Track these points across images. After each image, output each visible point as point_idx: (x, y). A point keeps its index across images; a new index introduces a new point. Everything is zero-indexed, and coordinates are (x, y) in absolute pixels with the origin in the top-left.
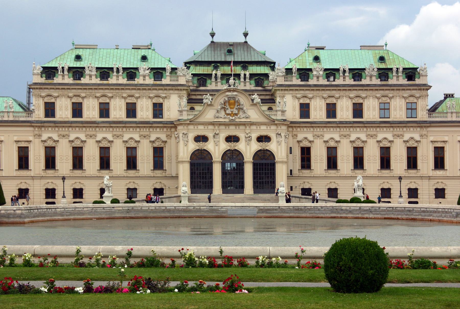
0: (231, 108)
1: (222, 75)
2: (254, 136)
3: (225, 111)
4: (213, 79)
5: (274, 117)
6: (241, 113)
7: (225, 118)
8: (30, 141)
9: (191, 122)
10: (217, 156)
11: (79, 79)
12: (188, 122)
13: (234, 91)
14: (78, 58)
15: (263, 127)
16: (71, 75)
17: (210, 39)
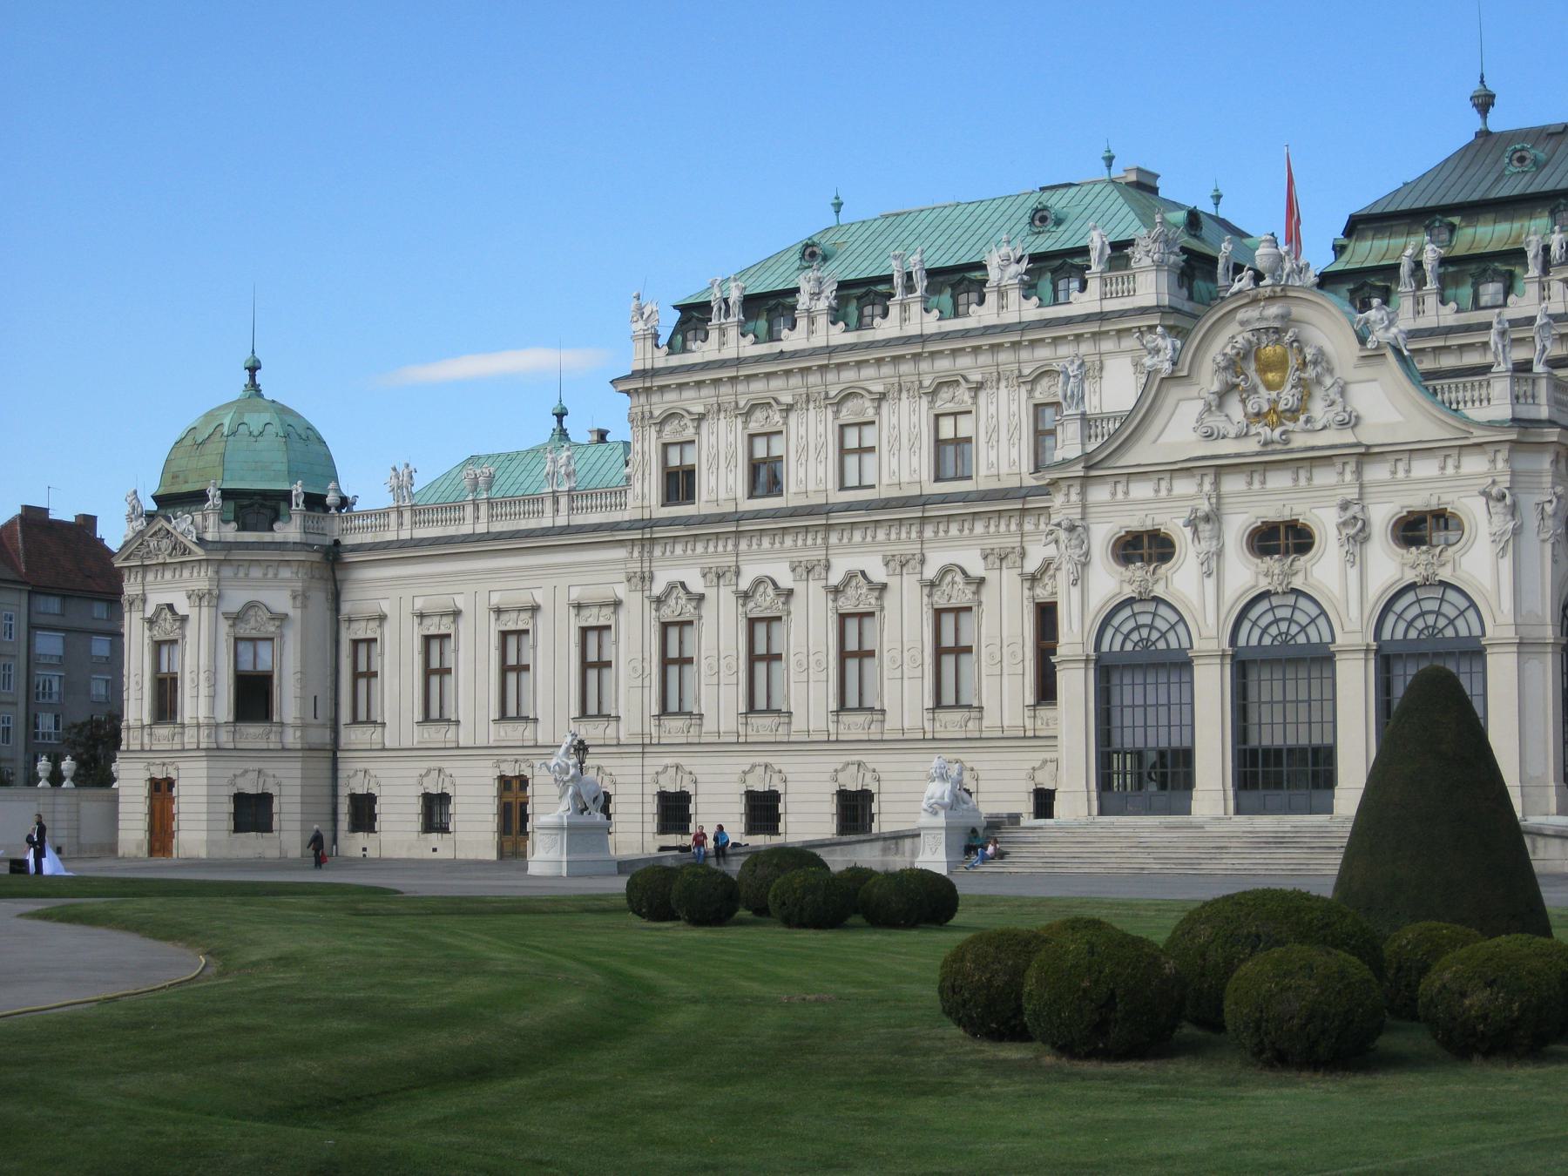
0: (1269, 387)
1: (1443, 262)
2: (1382, 515)
3: (1243, 401)
4: (1405, 286)
5: (1476, 413)
6: (1318, 409)
7: (1237, 437)
8: (617, 604)
9: (1092, 468)
10: (1207, 633)
11: (772, 337)
12: (1078, 470)
13: (1272, 298)
14: (811, 253)
15: (1425, 468)
16: (762, 324)
17: (1474, 123)
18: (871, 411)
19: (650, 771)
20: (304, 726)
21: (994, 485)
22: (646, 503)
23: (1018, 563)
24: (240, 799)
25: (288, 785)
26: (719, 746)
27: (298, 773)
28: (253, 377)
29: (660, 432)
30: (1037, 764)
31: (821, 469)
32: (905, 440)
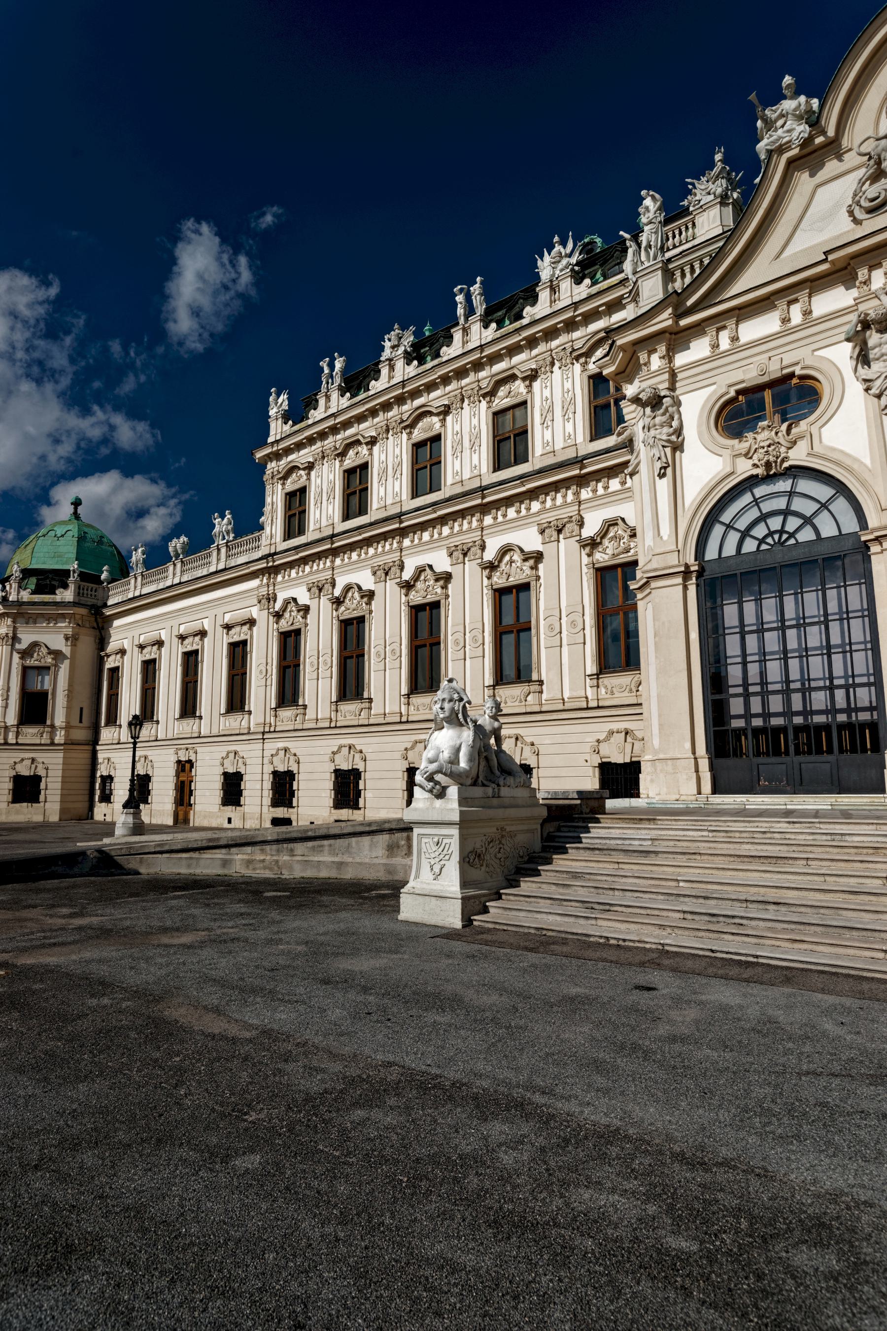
12: (664, 320)
18: (438, 425)
19: (267, 754)
20: (68, 727)
21: (550, 461)
22: (273, 541)
23: (576, 532)
24: (18, 780)
25: (52, 767)
26: (317, 731)
27: (61, 761)
28: (76, 509)
29: (283, 484)
30: (602, 737)
31: (397, 484)
32: (466, 443)
